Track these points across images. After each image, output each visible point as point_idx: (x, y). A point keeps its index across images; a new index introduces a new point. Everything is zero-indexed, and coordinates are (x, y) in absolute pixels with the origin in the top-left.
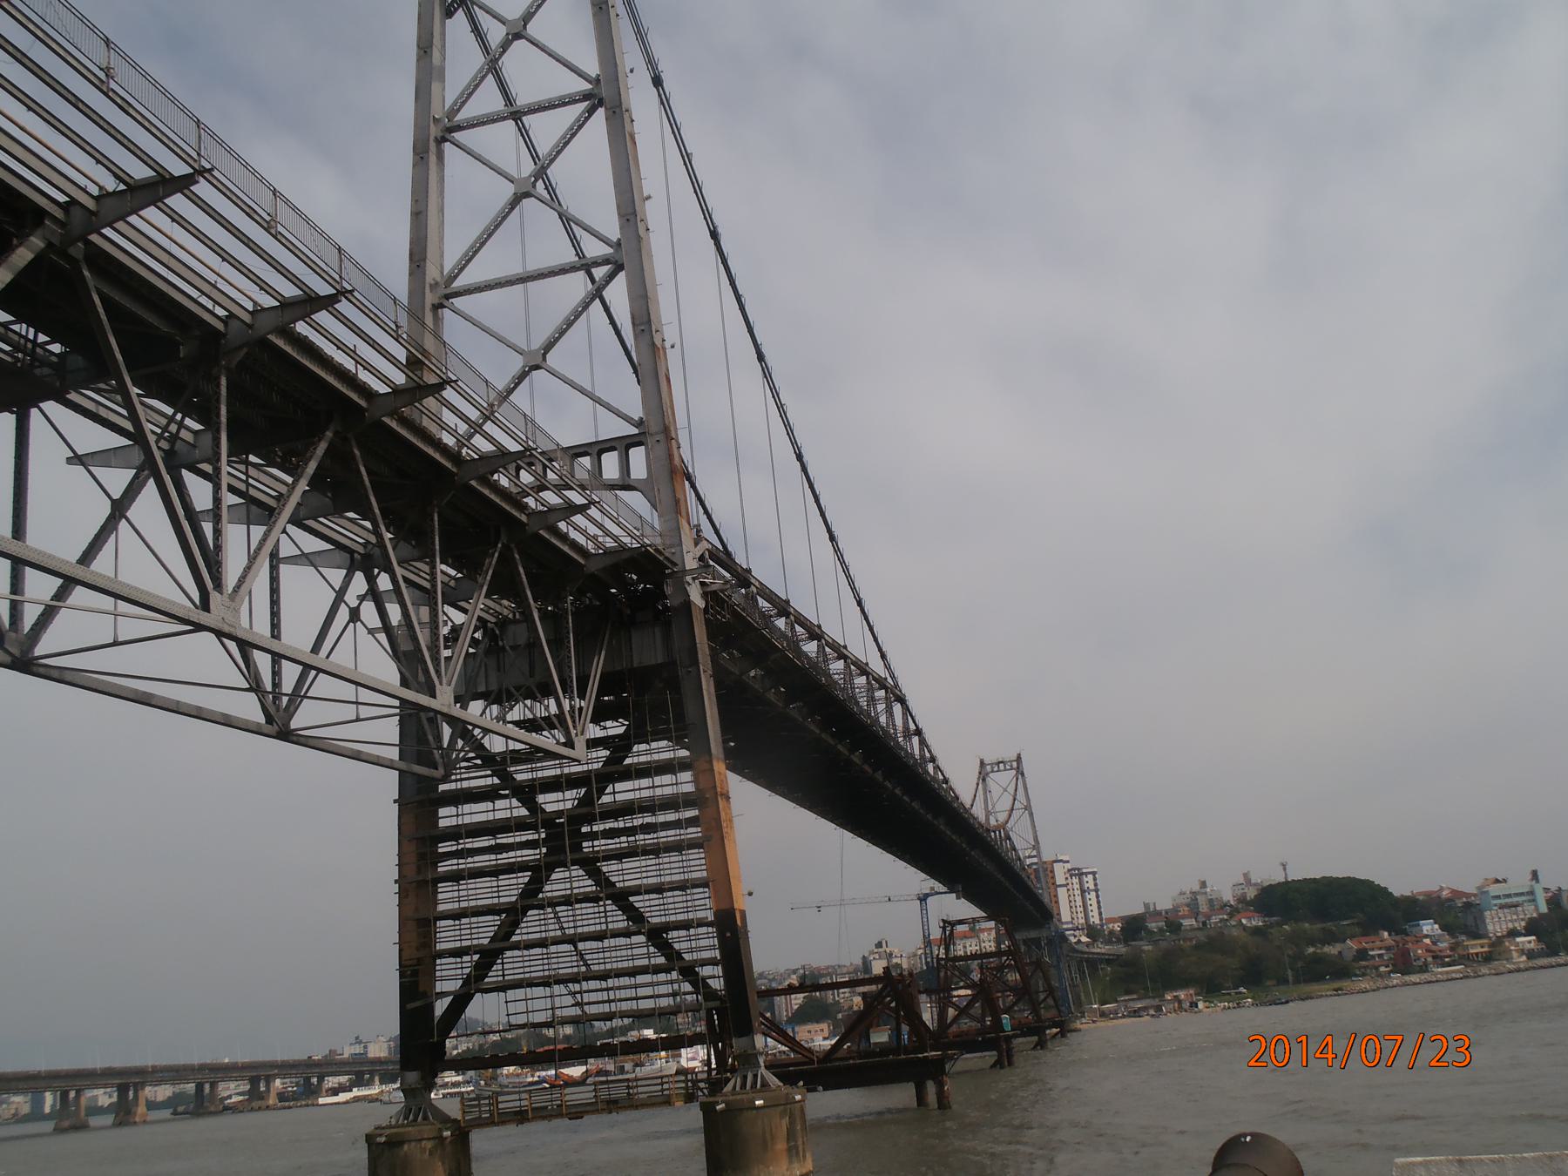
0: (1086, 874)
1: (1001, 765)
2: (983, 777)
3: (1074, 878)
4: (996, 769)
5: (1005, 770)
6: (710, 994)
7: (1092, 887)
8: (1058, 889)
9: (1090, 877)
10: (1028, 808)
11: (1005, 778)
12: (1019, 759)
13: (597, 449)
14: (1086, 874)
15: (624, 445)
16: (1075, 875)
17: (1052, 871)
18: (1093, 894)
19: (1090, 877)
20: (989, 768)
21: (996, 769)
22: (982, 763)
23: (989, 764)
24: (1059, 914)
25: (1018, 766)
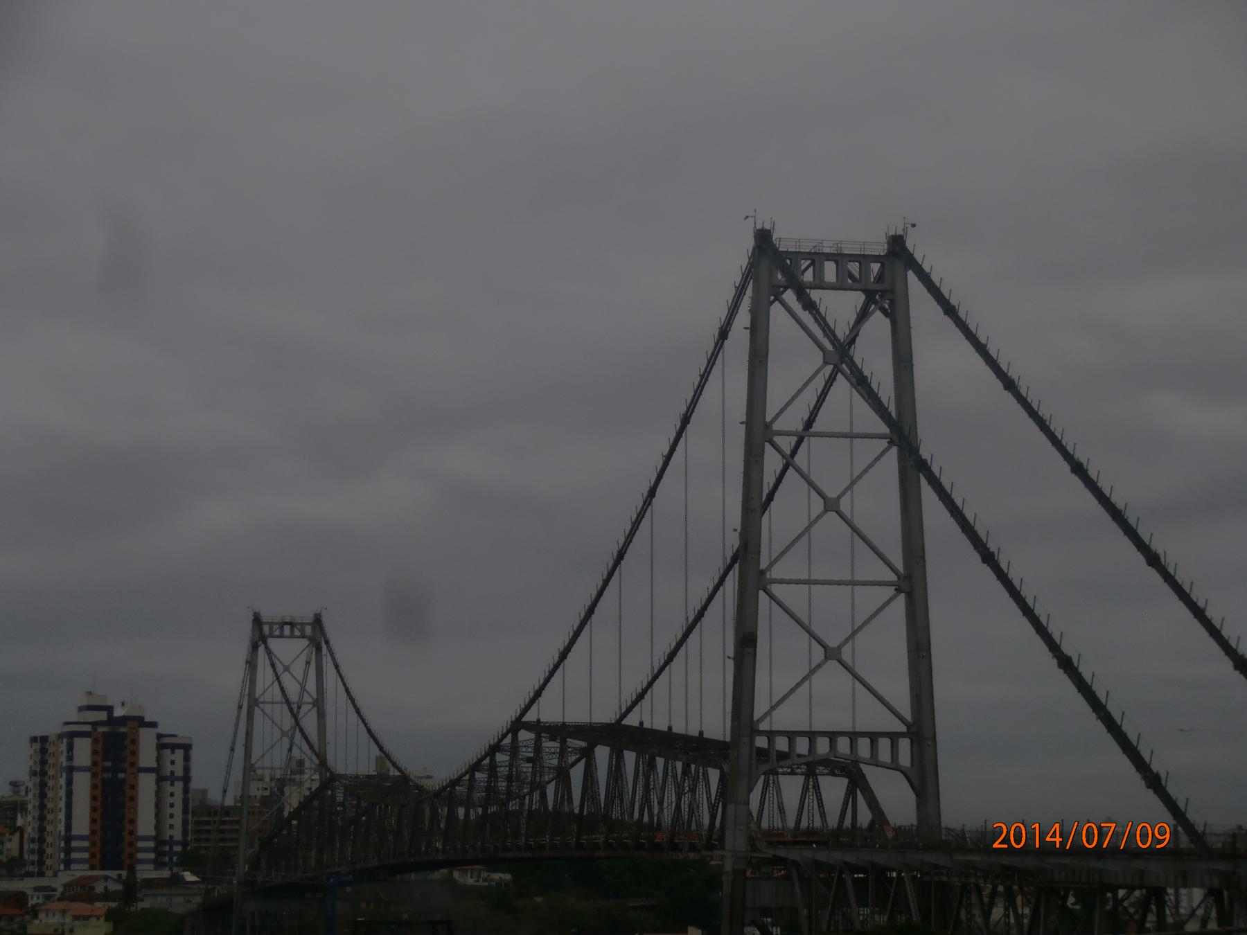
0: (174, 747)
1: (287, 629)
5: (292, 636)
7: (179, 772)
8: (142, 776)
9: (179, 754)
11: (289, 650)
12: (317, 621)
13: (874, 737)
14: (174, 747)
15: (894, 737)
18: (179, 786)
19: (179, 754)
20: (266, 629)
22: (257, 621)
23: (266, 623)
24: (133, 821)
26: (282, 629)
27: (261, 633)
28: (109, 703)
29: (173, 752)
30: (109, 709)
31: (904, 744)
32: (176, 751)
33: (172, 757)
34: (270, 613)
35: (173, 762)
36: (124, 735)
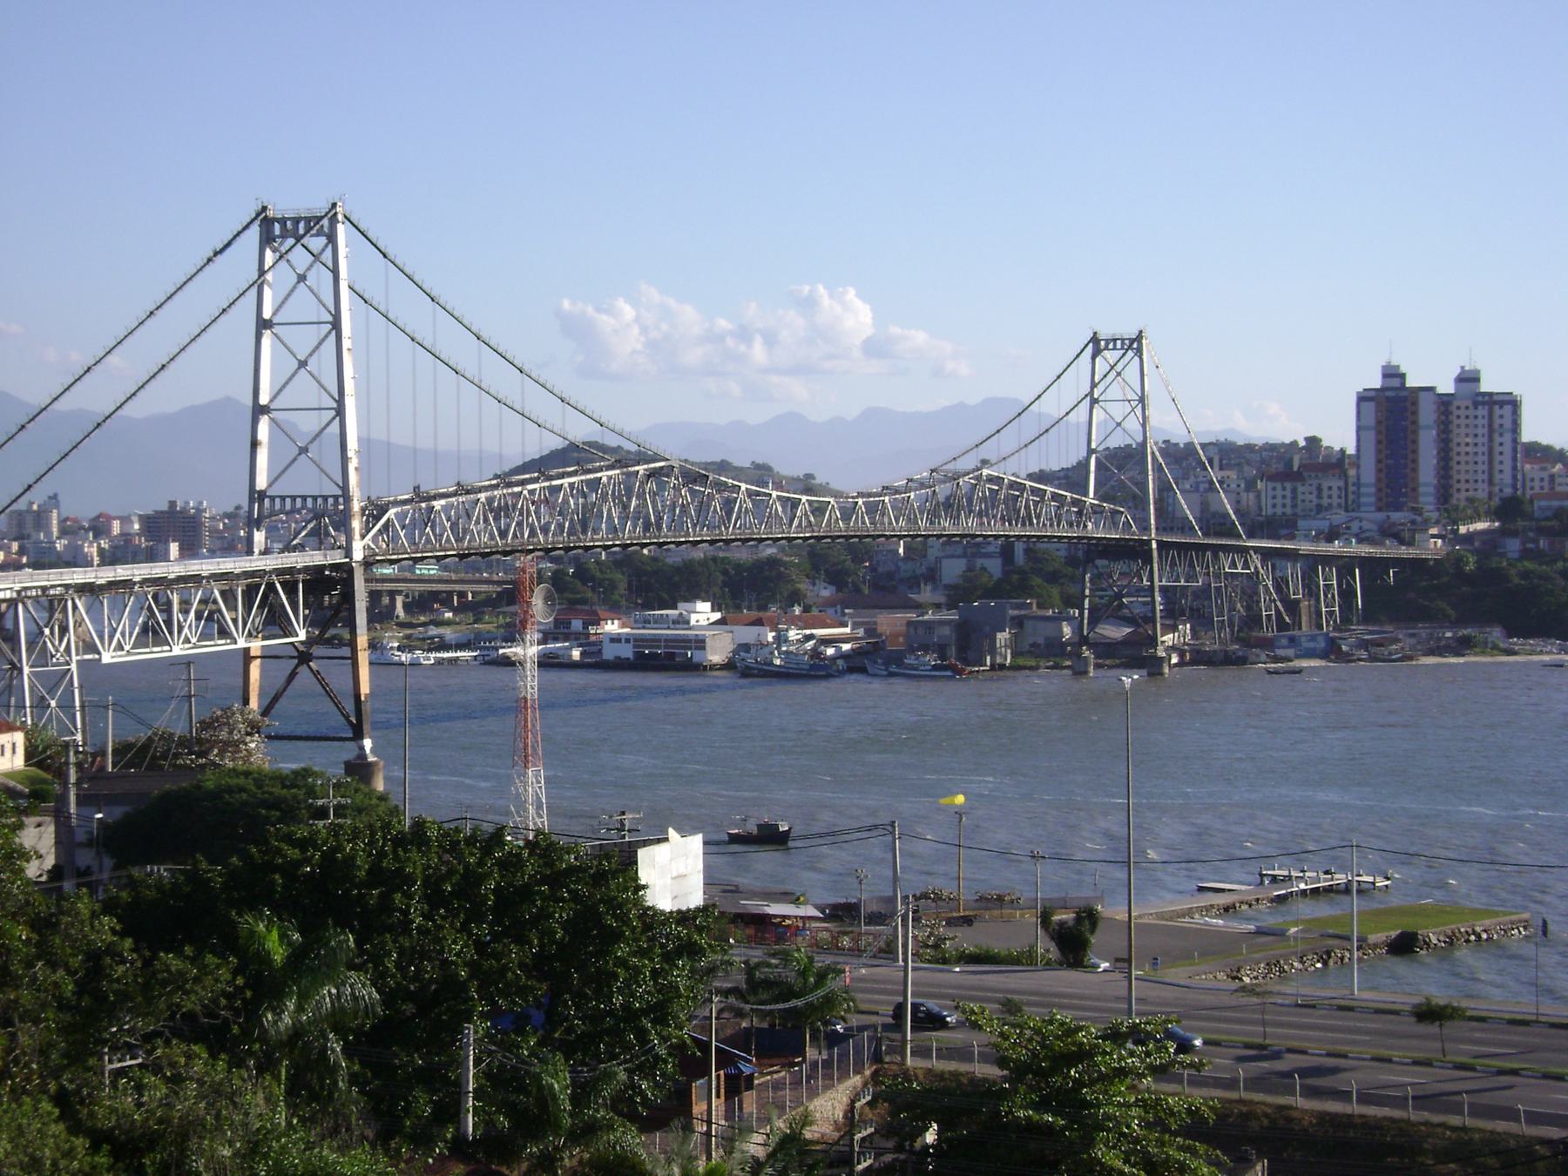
0: (1502, 404)
1: (1119, 342)
2: (1097, 353)
3: (1480, 407)
4: (1111, 346)
6: (350, 723)
7: (1508, 423)
9: (1508, 409)
10: (1142, 400)
15: (336, 498)
16: (1484, 403)
17: (1415, 403)
18: (1507, 438)
20: (1103, 343)
21: (1111, 346)
22: (1095, 340)
25: (1135, 343)
26: (1115, 345)
27: (1097, 345)
28: (1403, 369)
29: (1501, 407)
30: (1403, 376)
31: (341, 500)
32: (1505, 407)
33: (1501, 412)
34: (1104, 334)
35: (1501, 417)
36: (1405, 399)
